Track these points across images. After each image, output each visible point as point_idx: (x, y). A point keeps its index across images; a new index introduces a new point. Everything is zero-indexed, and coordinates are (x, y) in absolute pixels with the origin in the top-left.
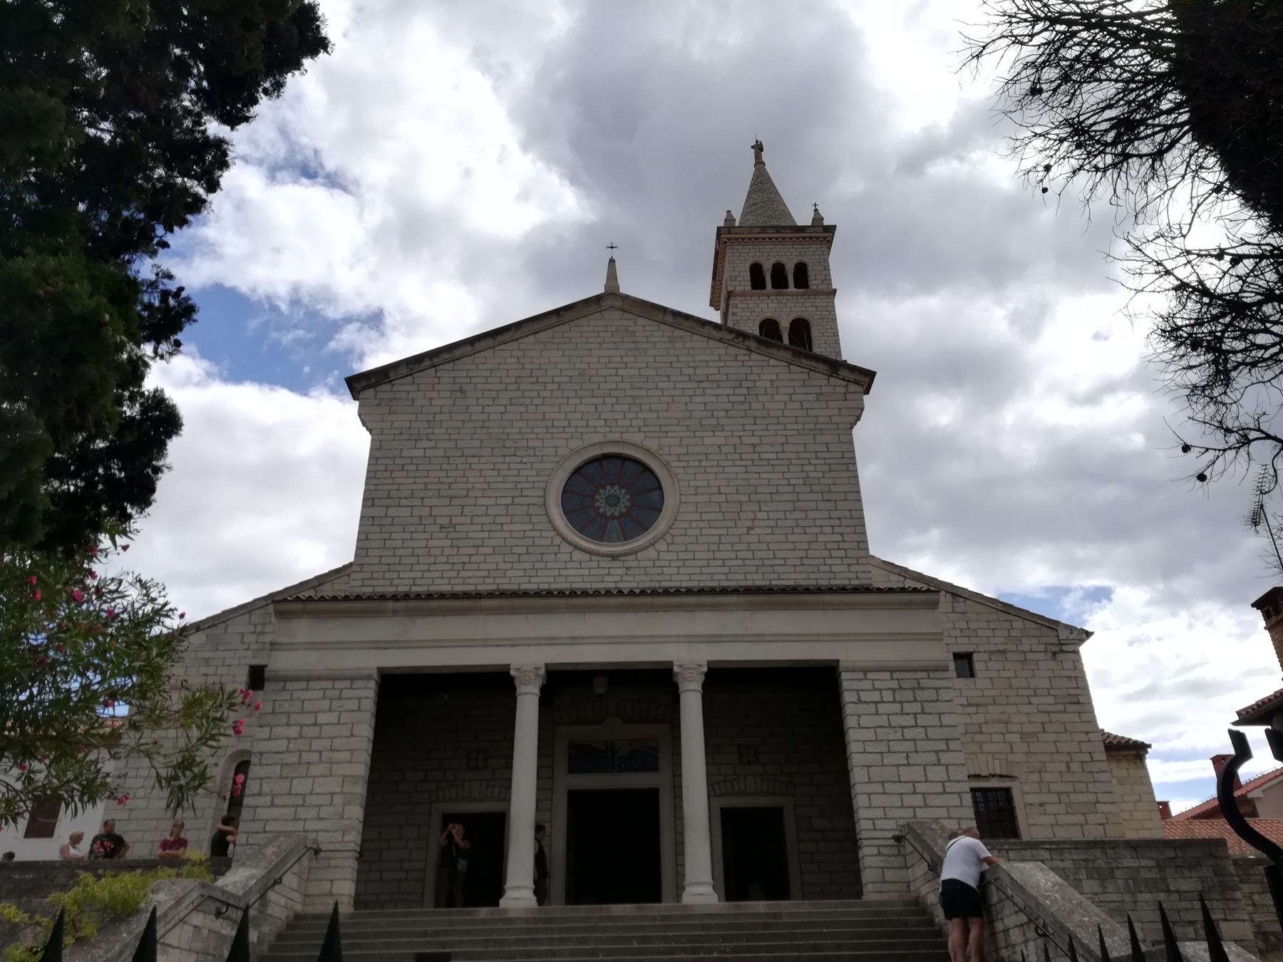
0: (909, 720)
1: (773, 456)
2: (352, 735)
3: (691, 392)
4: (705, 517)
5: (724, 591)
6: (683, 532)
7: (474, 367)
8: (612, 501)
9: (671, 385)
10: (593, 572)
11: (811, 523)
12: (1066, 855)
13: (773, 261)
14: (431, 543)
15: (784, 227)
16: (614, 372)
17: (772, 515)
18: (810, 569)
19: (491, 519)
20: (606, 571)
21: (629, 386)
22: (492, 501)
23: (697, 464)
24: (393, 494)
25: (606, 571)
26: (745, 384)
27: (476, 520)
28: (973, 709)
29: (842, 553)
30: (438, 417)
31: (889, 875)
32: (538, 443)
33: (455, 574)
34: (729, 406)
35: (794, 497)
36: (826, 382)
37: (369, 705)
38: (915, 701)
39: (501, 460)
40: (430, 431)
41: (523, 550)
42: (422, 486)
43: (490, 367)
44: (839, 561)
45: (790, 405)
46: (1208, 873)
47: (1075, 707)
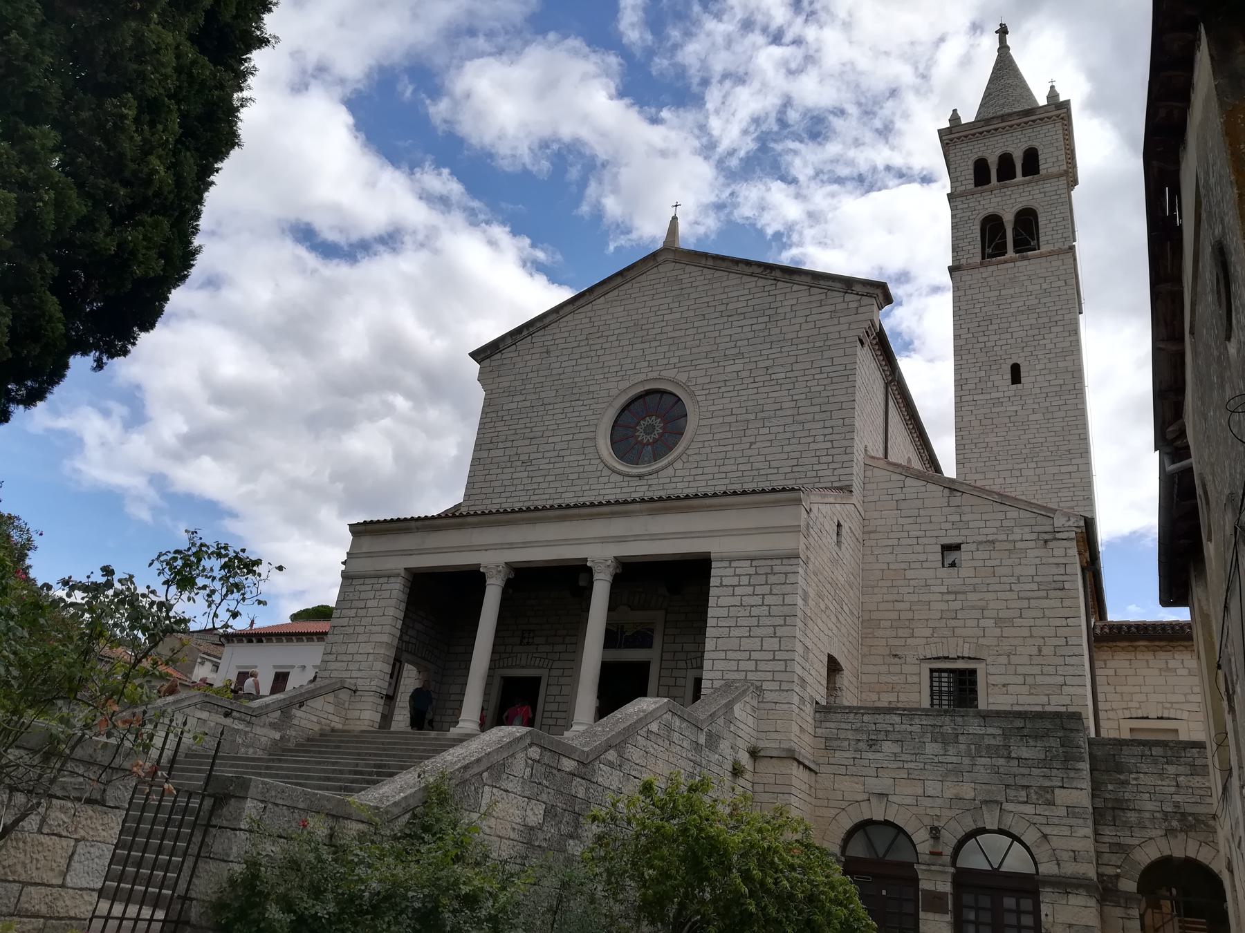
1: (783, 375)
3: (721, 327)
12: (917, 721)
13: (999, 152)
15: (1009, 115)
17: (774, 430)
18: (798, 475)
19: (555, 453)
26: (767, 312)
28: (952, 597)
45: (804, 326)
46: (1054, 743)
47: (1059, 593)
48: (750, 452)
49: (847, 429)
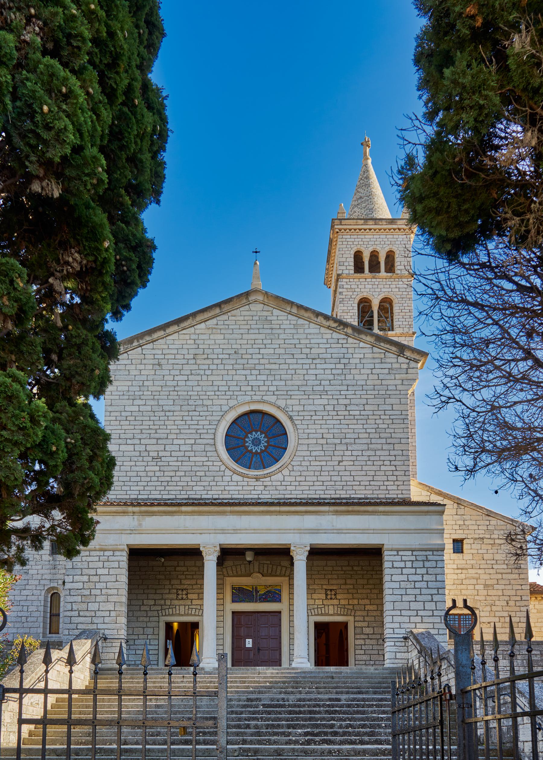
0: (419, 578)
1: (358, 413)
2: (117, 581)
3: (307, 367)
4: (314, 454)
5: (320, 503)
6: (299, 463)
7: (166, 347)
8: (256, 442)
9: (294, 361)
10: (245, 488)
11: (378, 458)
14: (148, 469)
16: (257, 351)
17: (355, 453)
19: (182, 454)
20: (252, 488)
21: (267, 361)
22: (182, 442)
23: (309, 418)
24: (122, 436)
25: (252, 488)
26: (343, 361)
27: (173, 454)
29: (394, 478)
30: (146, 383)
31: (399, 655)
32: (209, 402)
33: (163, 488)
34: (331, 377)
35: (368, 441)
36: (395, 360)
37: (125, 564)
38: (424, 567)
39: (186, 414)
40: (141, 393)
41: (202, 474)
42: (139, 431)
43: (177, 346)
44: (392, 483)
45: (371, 377)
48: (337, 468)
49: (404, 458)
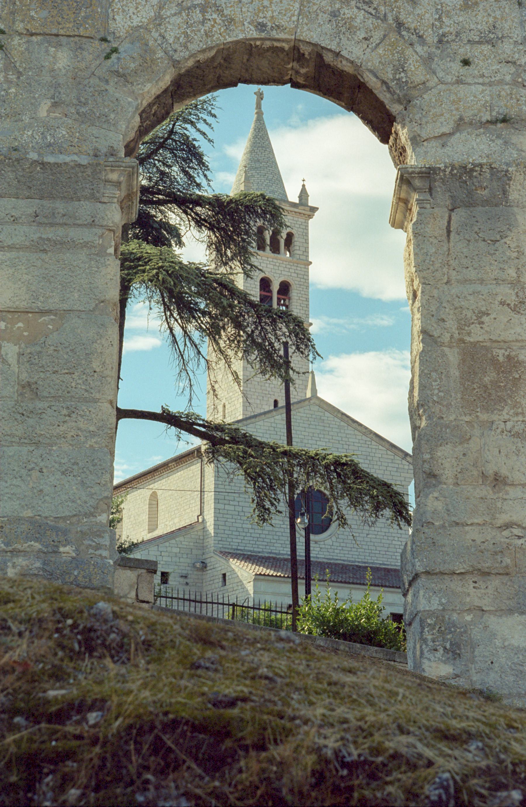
16: (314, 442)
48: (366, 539)
